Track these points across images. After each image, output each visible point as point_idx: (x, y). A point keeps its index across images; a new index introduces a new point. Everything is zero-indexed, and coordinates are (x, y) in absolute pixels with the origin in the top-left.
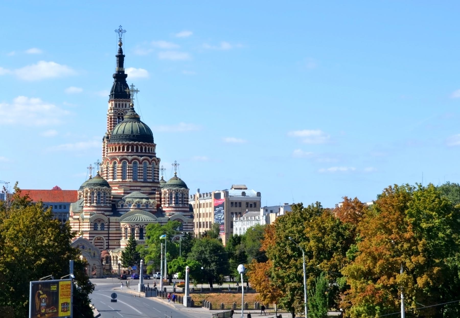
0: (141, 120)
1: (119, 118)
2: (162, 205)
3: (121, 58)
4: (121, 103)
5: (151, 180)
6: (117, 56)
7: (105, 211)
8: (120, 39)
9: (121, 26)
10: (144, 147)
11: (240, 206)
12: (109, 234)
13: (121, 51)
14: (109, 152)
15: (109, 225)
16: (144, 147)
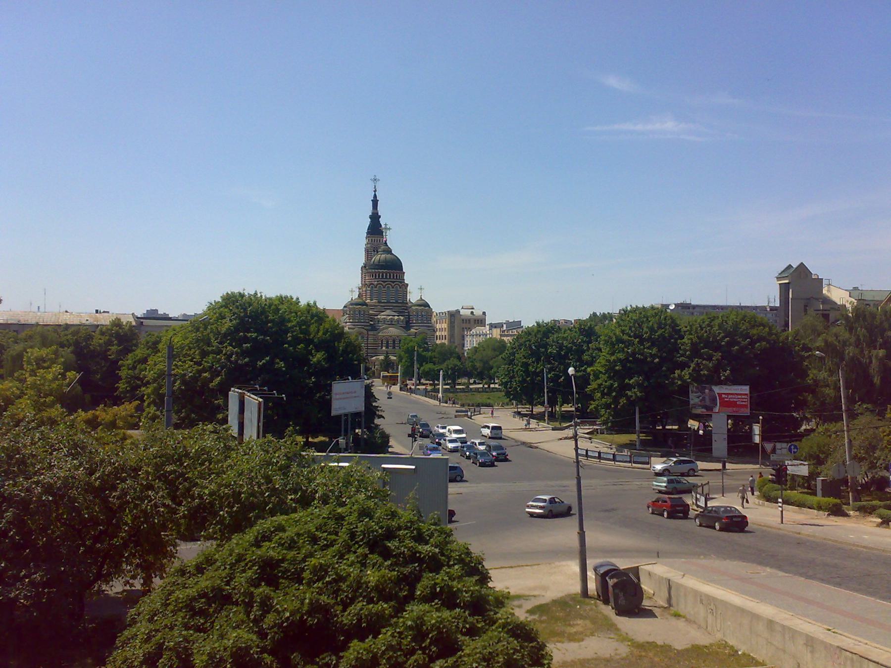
0: (393, 252)
1: (374, 251)
2: (411, 322)
3: (375, 202)
4: (376, 239)
5: (401, 301)
6: (372, 200)
7: (365, 326)
8: (375, 186)
9: (375, 176)
10: (395, 275)
11: (469, 323)
12: (368, 344)
13: (375, 196)
14: (367, 278)
15: (368, 337)
16: (395, 275)
